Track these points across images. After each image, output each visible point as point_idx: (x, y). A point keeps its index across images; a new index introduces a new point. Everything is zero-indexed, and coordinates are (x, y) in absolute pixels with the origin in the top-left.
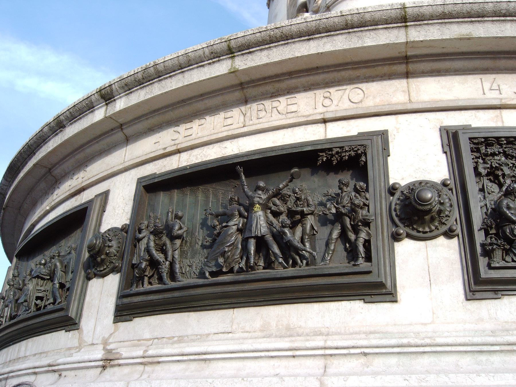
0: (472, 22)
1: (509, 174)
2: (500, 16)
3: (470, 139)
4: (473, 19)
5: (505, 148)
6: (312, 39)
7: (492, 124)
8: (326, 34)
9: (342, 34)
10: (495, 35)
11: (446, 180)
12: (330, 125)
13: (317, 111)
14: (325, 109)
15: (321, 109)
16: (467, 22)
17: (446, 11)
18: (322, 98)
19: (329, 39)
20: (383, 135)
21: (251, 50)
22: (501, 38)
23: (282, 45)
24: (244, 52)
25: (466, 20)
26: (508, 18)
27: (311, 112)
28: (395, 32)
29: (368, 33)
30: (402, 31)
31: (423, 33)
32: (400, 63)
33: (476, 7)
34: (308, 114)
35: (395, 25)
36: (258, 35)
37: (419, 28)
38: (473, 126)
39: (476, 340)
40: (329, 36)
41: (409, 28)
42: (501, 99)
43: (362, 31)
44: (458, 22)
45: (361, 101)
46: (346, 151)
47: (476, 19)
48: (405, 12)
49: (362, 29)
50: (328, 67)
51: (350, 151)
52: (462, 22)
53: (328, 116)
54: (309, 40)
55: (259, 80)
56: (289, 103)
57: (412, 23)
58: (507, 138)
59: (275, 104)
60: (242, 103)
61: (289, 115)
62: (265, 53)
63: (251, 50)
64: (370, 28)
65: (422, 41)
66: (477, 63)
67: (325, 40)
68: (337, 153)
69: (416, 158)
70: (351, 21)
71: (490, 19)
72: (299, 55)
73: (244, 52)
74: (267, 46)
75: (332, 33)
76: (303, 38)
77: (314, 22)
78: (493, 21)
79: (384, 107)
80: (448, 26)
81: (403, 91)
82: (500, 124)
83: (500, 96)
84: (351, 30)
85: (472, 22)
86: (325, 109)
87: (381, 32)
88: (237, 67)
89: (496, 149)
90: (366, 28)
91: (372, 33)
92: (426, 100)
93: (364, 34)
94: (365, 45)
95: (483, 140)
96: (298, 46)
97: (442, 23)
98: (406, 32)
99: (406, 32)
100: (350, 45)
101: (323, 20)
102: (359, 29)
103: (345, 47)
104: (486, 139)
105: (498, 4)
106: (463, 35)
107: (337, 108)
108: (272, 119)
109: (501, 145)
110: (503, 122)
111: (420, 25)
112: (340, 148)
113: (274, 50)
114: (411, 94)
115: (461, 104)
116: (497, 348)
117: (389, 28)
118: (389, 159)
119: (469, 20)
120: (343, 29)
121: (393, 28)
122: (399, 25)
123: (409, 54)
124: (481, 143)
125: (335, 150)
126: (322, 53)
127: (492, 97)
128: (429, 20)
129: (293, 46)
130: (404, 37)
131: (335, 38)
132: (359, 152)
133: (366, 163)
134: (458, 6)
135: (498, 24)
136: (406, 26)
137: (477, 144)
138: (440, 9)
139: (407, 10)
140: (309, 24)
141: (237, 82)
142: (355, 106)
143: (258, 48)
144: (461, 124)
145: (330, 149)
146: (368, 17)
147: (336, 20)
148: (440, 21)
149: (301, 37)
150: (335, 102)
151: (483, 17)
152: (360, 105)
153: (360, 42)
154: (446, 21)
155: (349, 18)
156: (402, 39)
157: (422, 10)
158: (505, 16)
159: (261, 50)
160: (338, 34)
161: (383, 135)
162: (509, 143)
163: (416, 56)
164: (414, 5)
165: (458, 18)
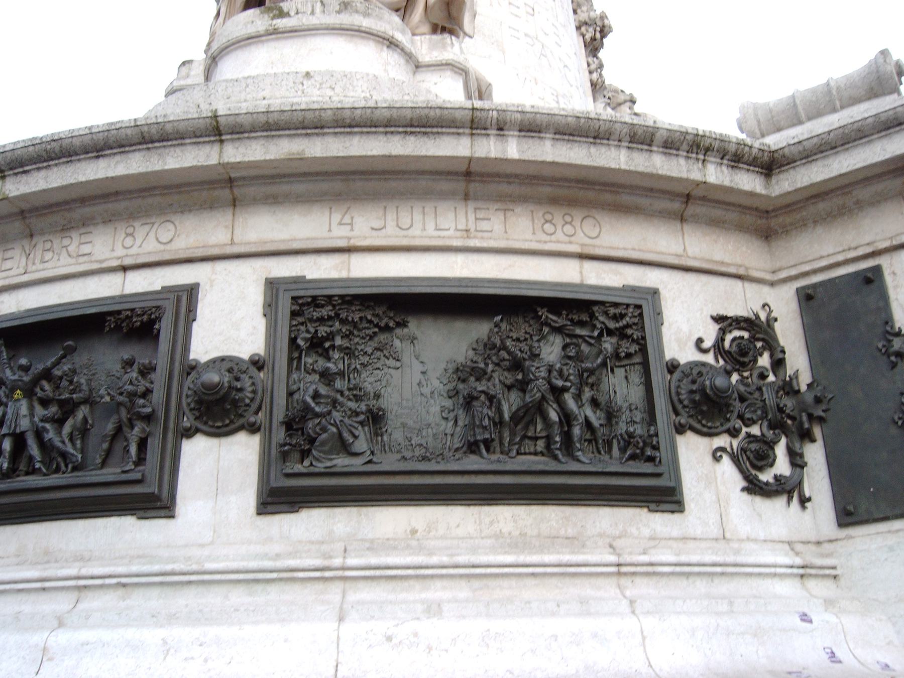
0: (307, 134)
1: (340, 346)
2: (344, 127)
3: (293, 298)
4: (309, 131)
5: (339, 309)
6: (102, 156)
7: (334, 275)
8: (119, 150)
9: (139, 150)
10: (335, 154)
11: (257, 354)
12: (131, 276)
13: (115, 254)
14: (125, 252)
15: (120, 252)
16: (301, 135)
17: (270, 120)
18: (123, 235)
19: (123, 156)
20: (191, 292)
21: (26, 168)
22: (343, 157)
23: (64, 163)
24: (16, 171)
25: (299, 132)
26: (356, 130)
27: (108, 255)
28: (207, 149)
29: (172, 149)
30: (216, 147)
31: (242, 150)
32: (222, 188)
33: (309, 115)
34: (103, 257)
35: (207, 139)
36: (31, 149)
37: (237, 144)
38: (309, 277)
39: (253, 565)
40: (122, 152)
41: (225, 144)
42: (349, 239)
43: (164, 146)
44: (289, 136)
45: (171, 241)
46: (138, 315)
47: (313, 131)
48: (217, 122)
49: (165, 143)
50: (130, 192)
51: (143, 315)
52: (295, 135)
53: (128, 262)
54: (98, 157)
55: (45, 207)
56: (82, 241)
57: (229, 137)
58: (342, 297)
59: (66, 242)
60: (26, 237)
61: (81, 259)
62: (43, 173)
63: (26, 168)
64: (174, 142)
65: (239, 163)
66: (325, 186)
67: (118, 158)
68: (127, 317)
69: (230, 324)
70: (149, 132)
71: (331, 130)
72: (84, 179)
73: (16, 171)
74: (45, 164)
75: (127, 149)
76: (90, 155)
77: (101, 134)
78: (336, 133)
79: (196, 251)
80: (276, 141)
81: (226, 227)
82: (344, 275)
83: (350, 234)
84: (150, 146)
85: (307, 134)
86: (125, 252)
87: (189, 148)
88: (7, 192)
89: (325, 312)
90: (170, 143)
91: (178, 150)
92: (253, 240)
93: (167, 150)
94: (166, 167)
95: (309, 300)
96: (83, 165)
97: (267, 136)
98: (221, 149)
99: (221, 149)
100: (147, 167)
101: (113, 132)
102: (161, 144)
103: (142, 170)
104: (314, 298)
105: (340, 112)
106: (293, 154)
107: (140, 251)
108: (59, 264)
109: (334, 306)
110: (349, 270)
111: (239, 139)
112: (132, 310)
113: (55, 169)
114: (235, 232)
115: (296, 246)
116: (274, 575)
117: (199, 143)
118: (195, 324)
119: (304, 132)
120: (140, 143)
121: (204, 142)
122: (212, 139)
123: (233, 175)
124: (308, 304)
125: (124, 314)
126: (112, 178)
127: (339, 235)
128: (251, 131)
129: (78, 165)
130: (217, 156)
131: (130, 155)
132: (153, 316)
133: (159, 331)
134: (286, 114)
135: (341, 137)
136: (222, 141)
137: (303, 305)
138: (263, 119)
139: (219, 119)
140: (94, 136)
141: (16, 210)
142: (162, 247)
143: (34, 166)
144: (294, 274)
145: (119, 312)
146: (169, 127)
147: (129, 132)
148: (265, 134)
149: (87, 153)
150: (138, 242)
151: (322, 127)
152: (168, 247)
153: (160, 162)
154: (273, 133)
155: (146, 129)
156: (213, 161)
157: (239, 119)
158: (350, 126)
159: (39, 169)
160: (134, 151)
161: (191, 292)
162: (344, 302)
163: (244, 178)
164: (229, 112)
165: (289, 129)
